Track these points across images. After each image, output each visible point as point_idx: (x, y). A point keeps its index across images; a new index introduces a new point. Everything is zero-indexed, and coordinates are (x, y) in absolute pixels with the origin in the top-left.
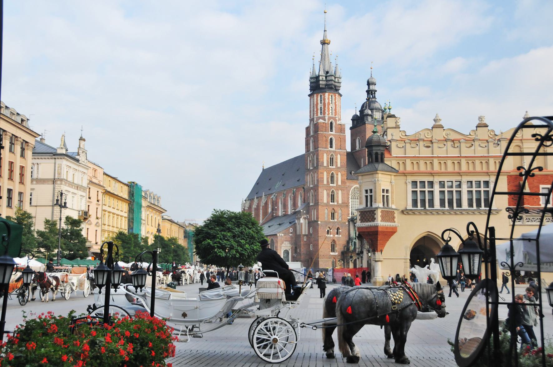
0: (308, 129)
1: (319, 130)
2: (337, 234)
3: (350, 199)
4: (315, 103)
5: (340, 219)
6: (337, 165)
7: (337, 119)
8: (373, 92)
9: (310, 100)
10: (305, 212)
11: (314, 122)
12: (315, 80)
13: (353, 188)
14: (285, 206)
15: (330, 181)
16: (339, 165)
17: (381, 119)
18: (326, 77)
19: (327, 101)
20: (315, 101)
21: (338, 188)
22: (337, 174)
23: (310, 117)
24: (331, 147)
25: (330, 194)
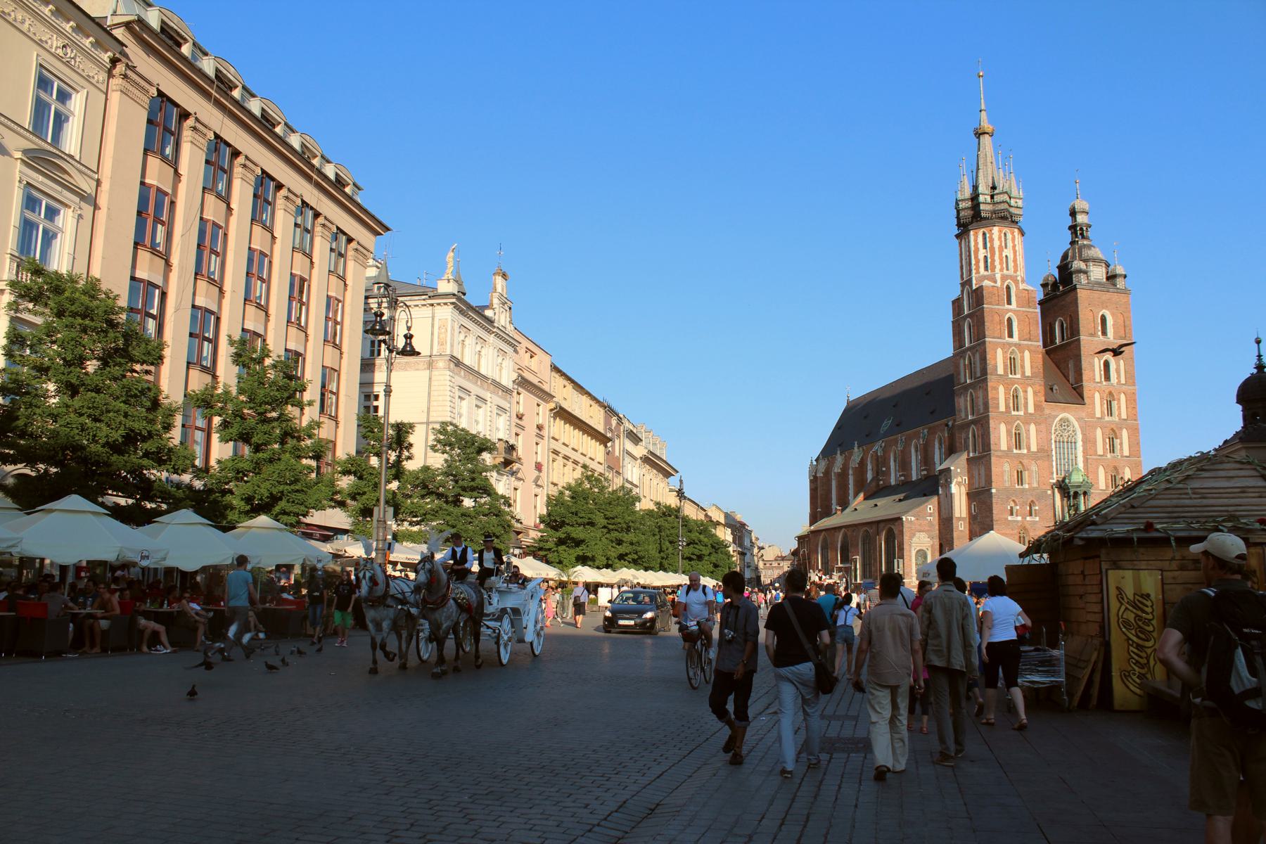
0: (957, 304)
1: (985, 302)
2: (1031, 515)
3: (1053, 441)
4: (973, 249)
5: (1035, 485)
6: (1023, 373)
7: (1019, 278)
8: (1085, 228)
9: (960, 244)
10: (959, 470)
11: (971, 286)
12: (970, 203)
13: (1058, 419)
14: (904, 465)
15: (1011, 405)
16: (1028, 373)
17: (1105, 280)
18: (992, 197)
19: (997, 243)
20: (972, 244)
21: (1028, 419)
22: (1026, 392)
23: (962, 278)
24: (1011, 335)
25: (1014, 431)
